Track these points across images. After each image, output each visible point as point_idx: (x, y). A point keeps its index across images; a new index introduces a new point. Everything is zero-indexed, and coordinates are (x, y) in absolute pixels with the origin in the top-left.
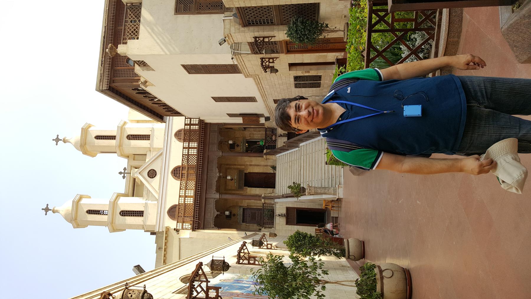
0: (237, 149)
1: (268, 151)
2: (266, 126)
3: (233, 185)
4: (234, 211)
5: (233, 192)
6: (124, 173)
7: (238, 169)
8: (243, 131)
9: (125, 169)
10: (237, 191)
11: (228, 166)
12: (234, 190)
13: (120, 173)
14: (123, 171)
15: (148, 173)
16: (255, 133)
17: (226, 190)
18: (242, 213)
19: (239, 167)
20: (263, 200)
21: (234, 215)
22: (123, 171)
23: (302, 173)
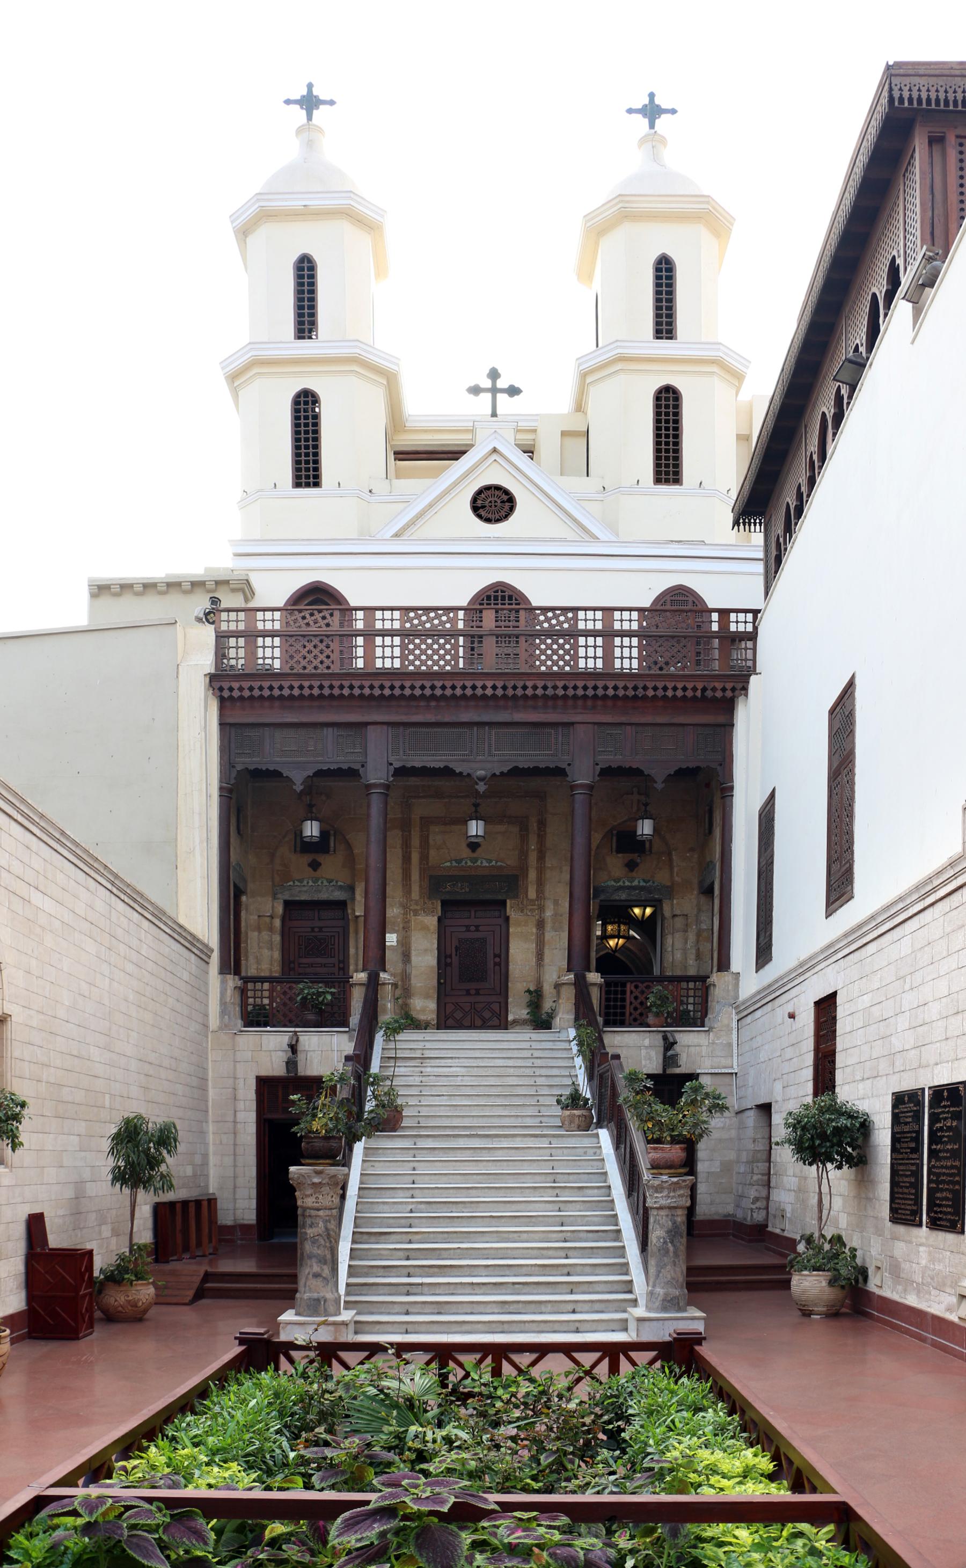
0: (615, 864)
1: (595, 994)
2: (715, 978)
3: (447, 851)
4: (332, 866)
5: (415, 857)
6: (494, 391)
7: (524, 870)
8: (701, 883)
9: (513, 391)
10: (422, 871)
11: (534, 826)
12: (424, 857)
13: (494, 375)
14: (502, 383)
15: (498, 488)
16: (692, 937)
17: (426, 822)
18: (324, 896)
19: (532, 875)
20: (362, 976)
21: (315, 865)
22: (502, 383)
23: (462, 1143)
